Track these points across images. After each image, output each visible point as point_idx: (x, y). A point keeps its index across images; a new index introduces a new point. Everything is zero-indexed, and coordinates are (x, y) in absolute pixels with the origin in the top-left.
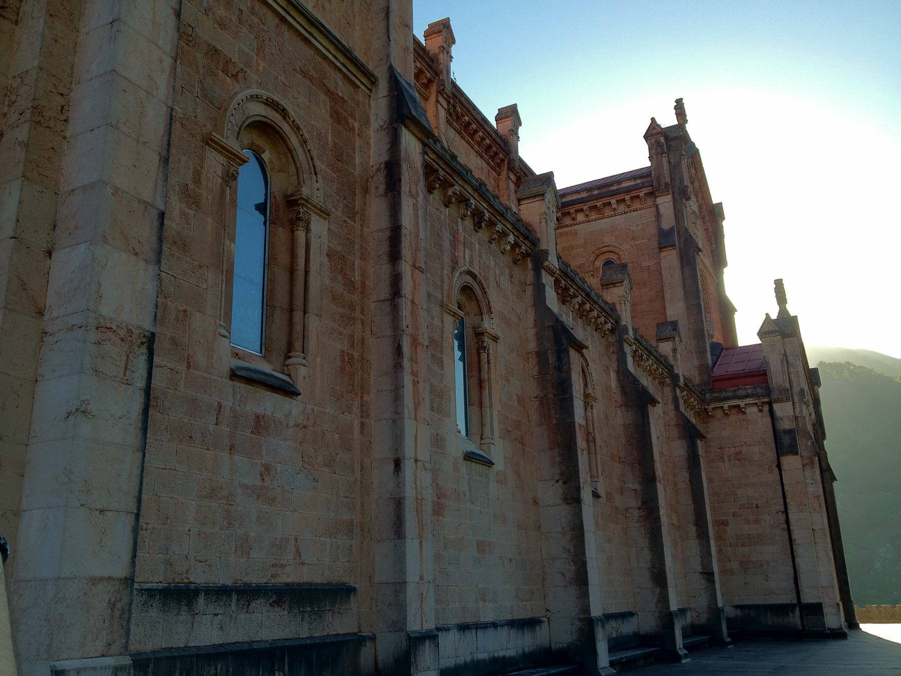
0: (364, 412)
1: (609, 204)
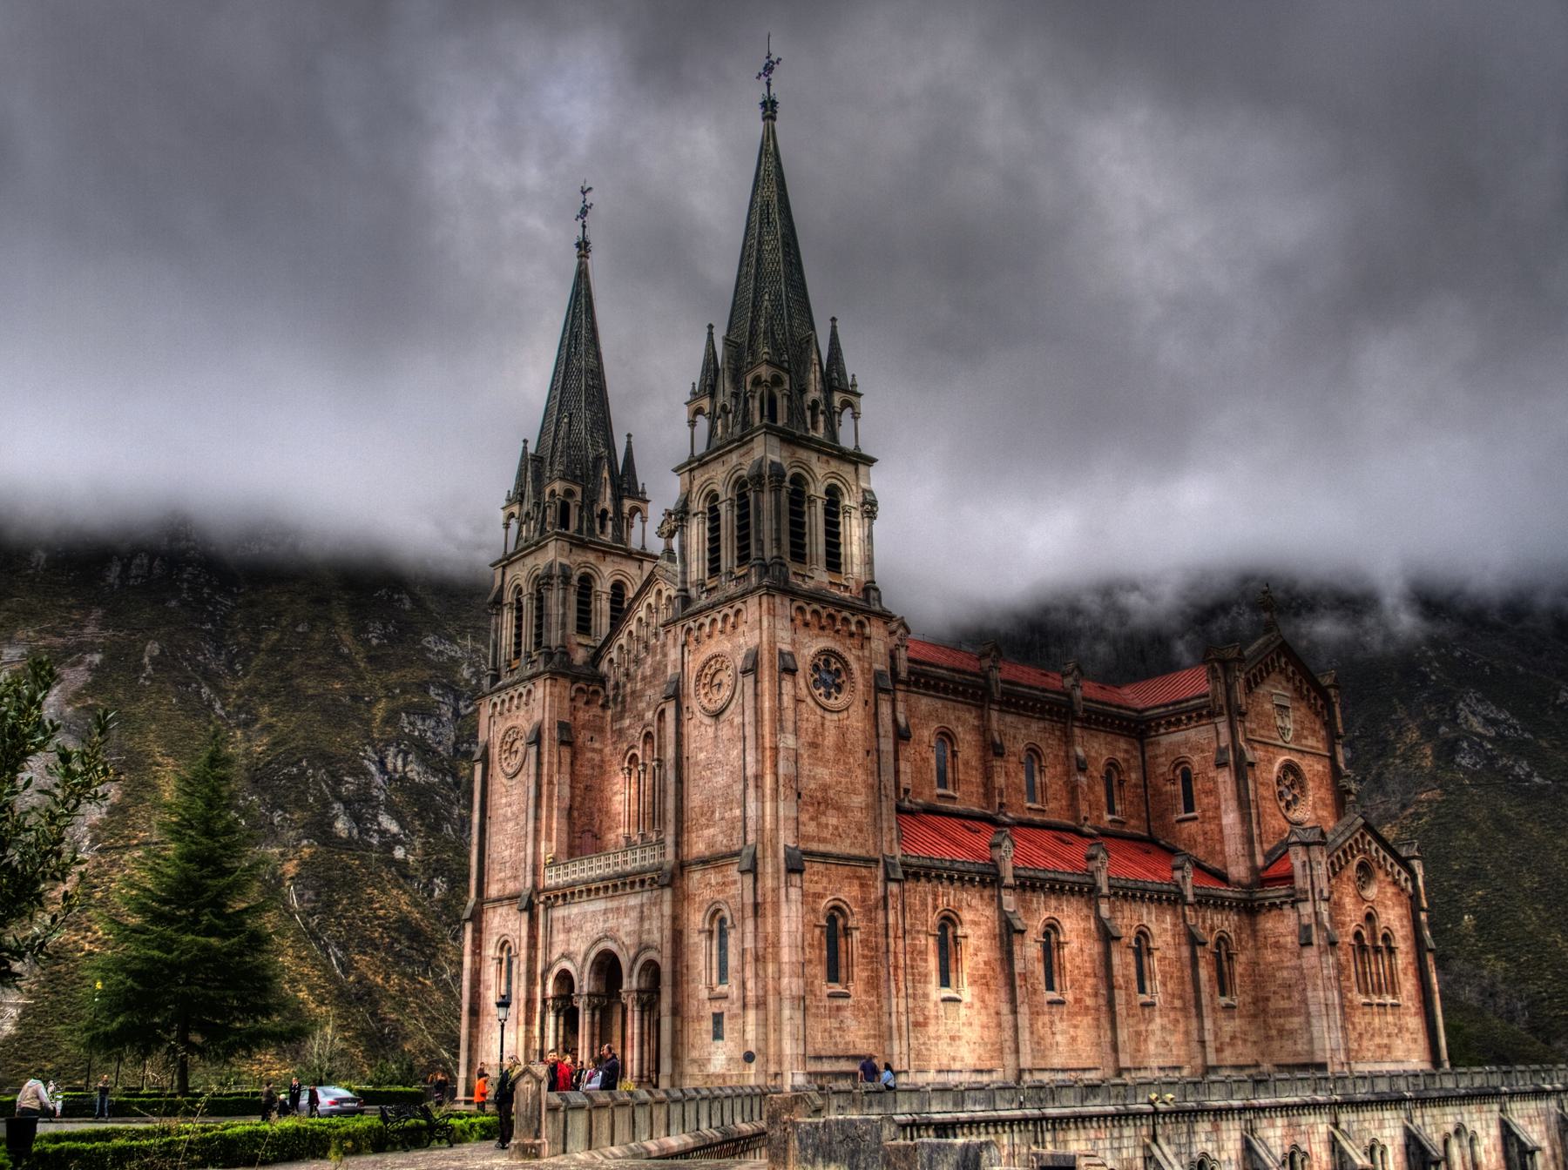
0: (879, 996)
1: (1180, 721)
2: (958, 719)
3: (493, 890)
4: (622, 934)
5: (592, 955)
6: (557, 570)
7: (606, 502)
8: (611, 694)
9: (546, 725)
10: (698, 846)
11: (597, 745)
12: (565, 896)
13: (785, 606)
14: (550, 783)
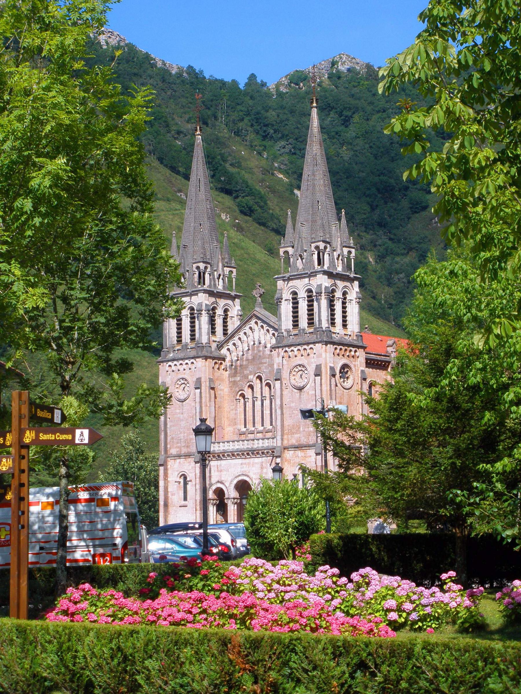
2: (378, 376)
3: (173, 451)
4: (251, 475)
5: (235, 482)
6: (204, 307)
7: (220, 272)
8: (228, 364)
9: (203, 380)
10: (294, 441)
11: (222, 388)
12: (219, 456)
13: (331, 348)
14: (206, 406)
